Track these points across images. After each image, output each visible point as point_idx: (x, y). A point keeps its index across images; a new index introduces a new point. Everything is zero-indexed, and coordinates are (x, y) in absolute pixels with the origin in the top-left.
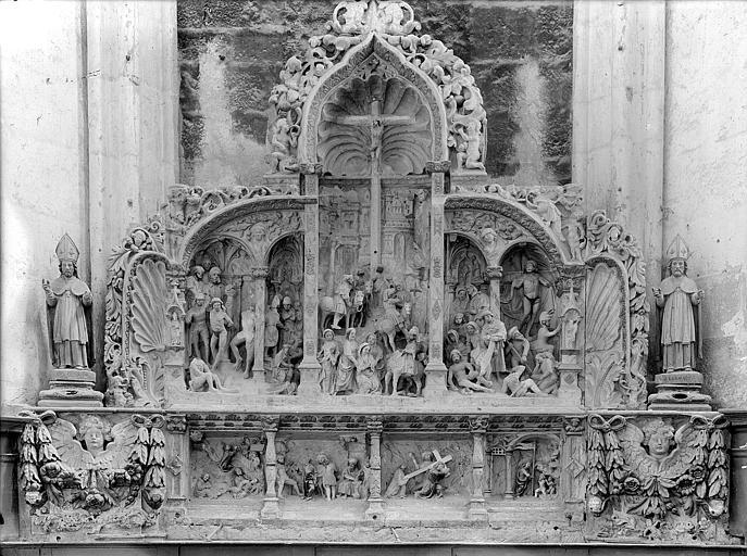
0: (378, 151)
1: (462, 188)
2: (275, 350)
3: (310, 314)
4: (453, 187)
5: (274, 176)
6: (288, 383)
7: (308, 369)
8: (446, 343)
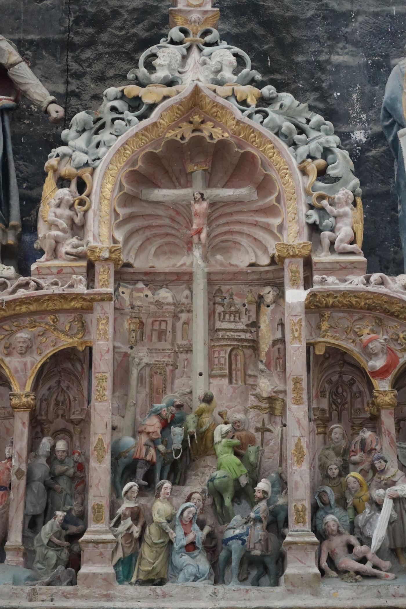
0: (203, 235)
1: (331, 279)
2: (40, 520)
3: (100, 460)
4: (316, 278)
5: (49, 263)
6: (61, 568)
7: (97, 543)
8: (315, 509)
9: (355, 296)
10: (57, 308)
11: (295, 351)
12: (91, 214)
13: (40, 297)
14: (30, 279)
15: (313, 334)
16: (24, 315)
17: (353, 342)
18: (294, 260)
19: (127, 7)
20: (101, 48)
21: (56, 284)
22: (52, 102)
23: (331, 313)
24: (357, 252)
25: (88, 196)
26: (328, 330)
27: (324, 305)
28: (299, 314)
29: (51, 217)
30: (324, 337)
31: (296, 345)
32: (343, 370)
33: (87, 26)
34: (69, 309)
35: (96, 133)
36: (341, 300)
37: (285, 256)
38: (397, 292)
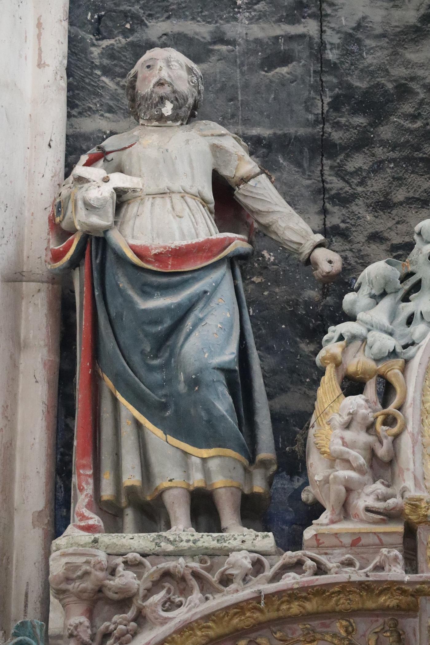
5: (337, 527)
10: (355, 606)
12: (406, 441)
13: (324, 588)
14: (305, 555)
16: (295, 619)
19: (424, 78)
20: (380, 152)
21: (350, 564)
22: (320, 245)
25: (400, 408)
29: (337, 446)
33: (354, 112)
34: (374, 610)
35: (406, 299)
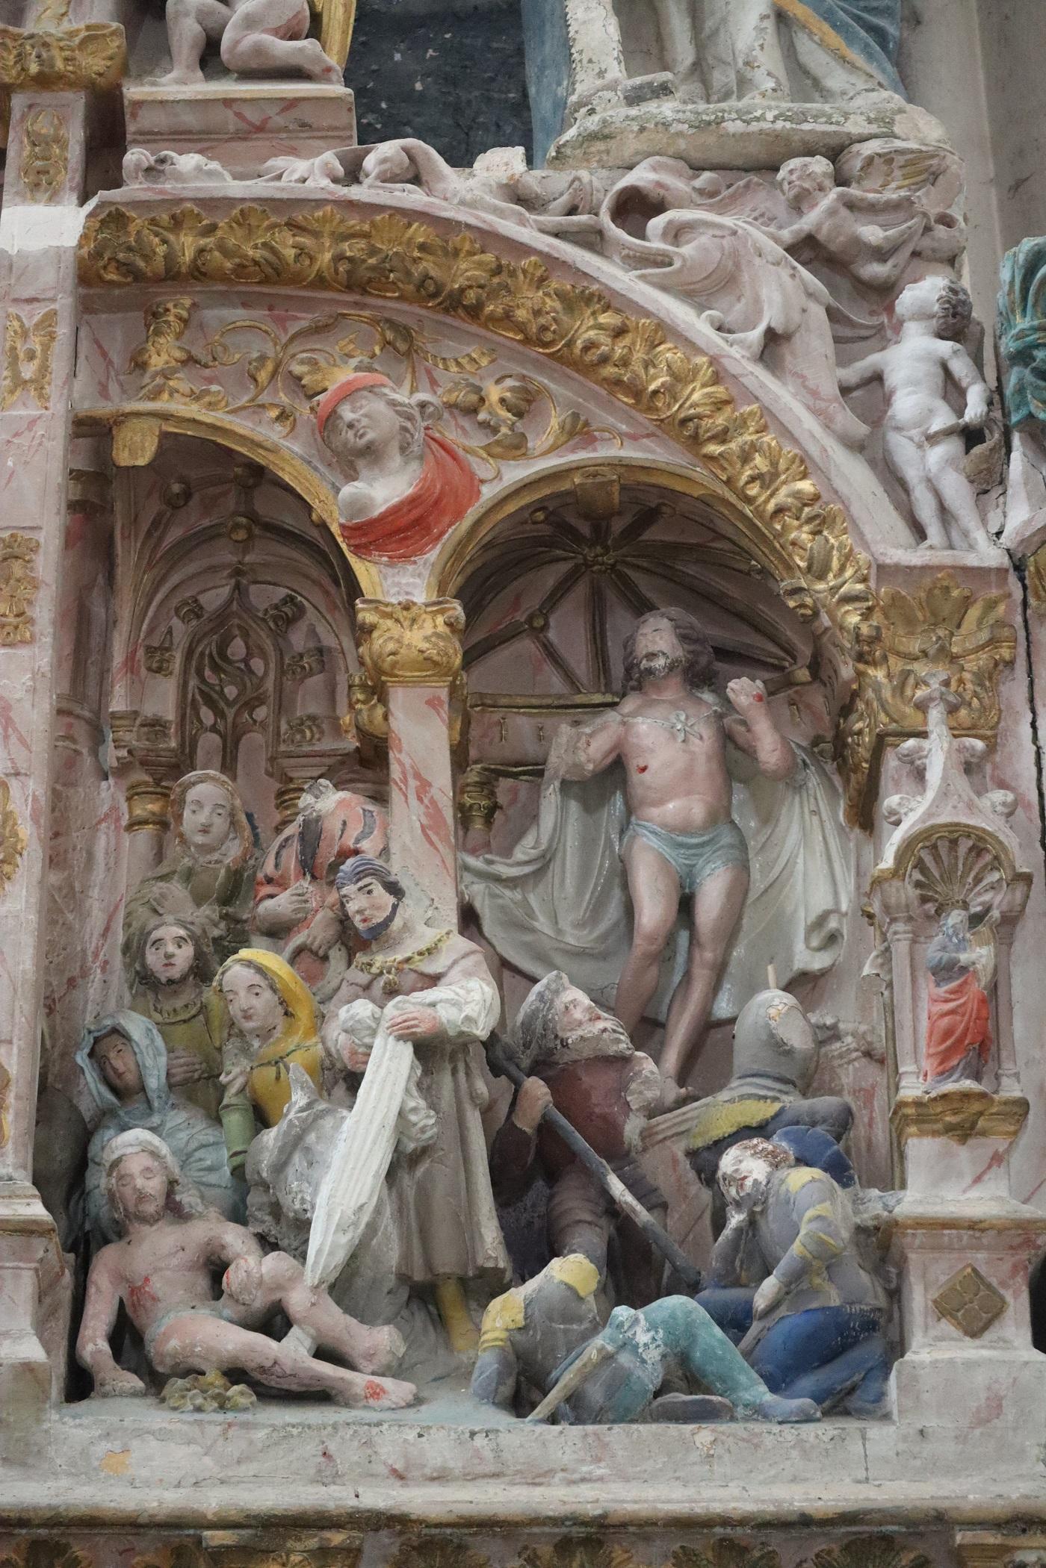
1: (188, 162)
4: (135, 156)
9: (292, 225)
11: (16, 435)
15: (114, 388)
17: (283, 416)
18: (46, 98)
23: (194, 305)
24: (317, 69)
26: (175, 371)
27: (159, 264)
28: (50, 294)
30: (155, 395)
31: (23, 412)
32: (248, 559)
36: (232, 241)
37: (7, 80)
38: (472, 204)
